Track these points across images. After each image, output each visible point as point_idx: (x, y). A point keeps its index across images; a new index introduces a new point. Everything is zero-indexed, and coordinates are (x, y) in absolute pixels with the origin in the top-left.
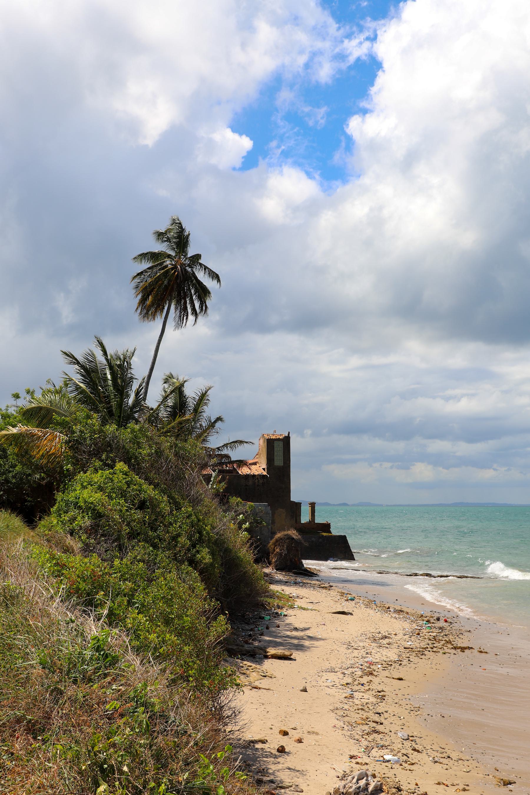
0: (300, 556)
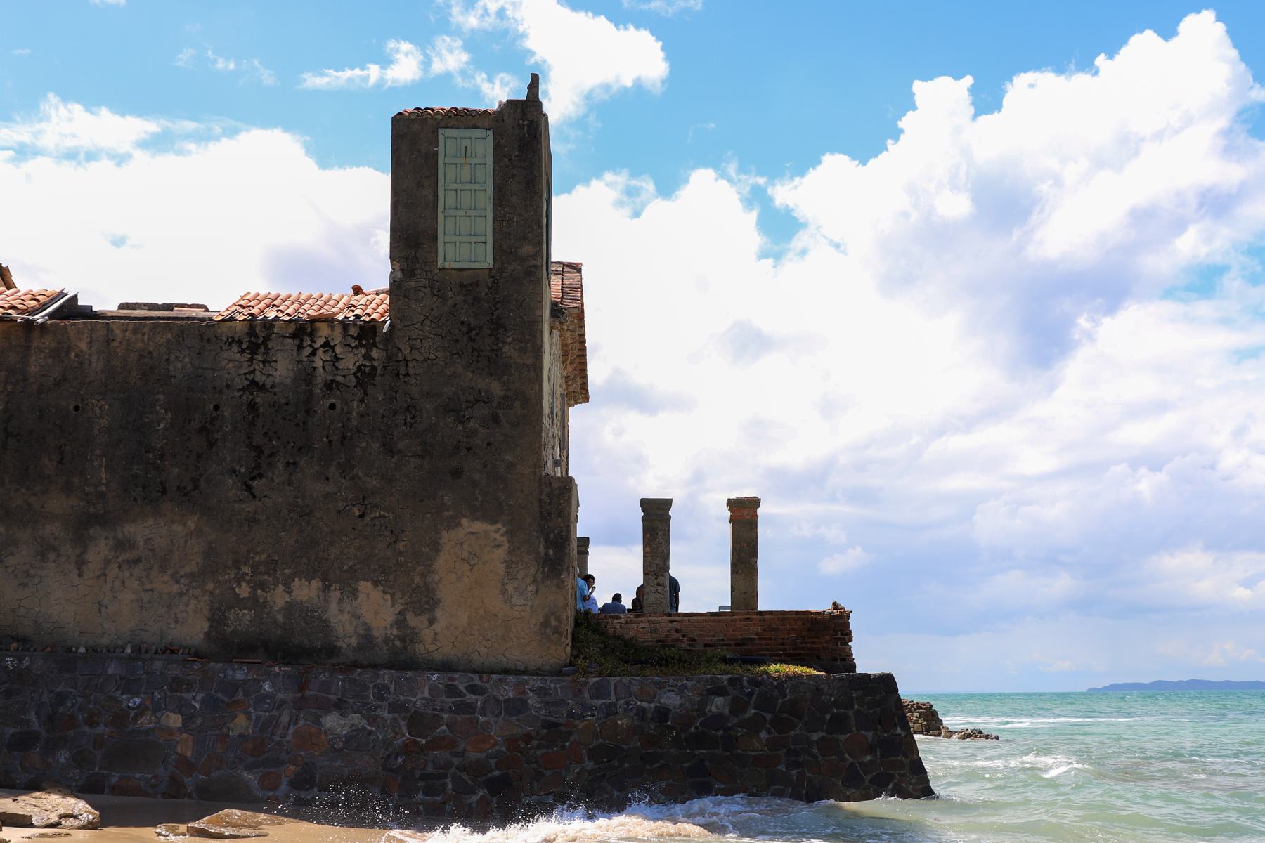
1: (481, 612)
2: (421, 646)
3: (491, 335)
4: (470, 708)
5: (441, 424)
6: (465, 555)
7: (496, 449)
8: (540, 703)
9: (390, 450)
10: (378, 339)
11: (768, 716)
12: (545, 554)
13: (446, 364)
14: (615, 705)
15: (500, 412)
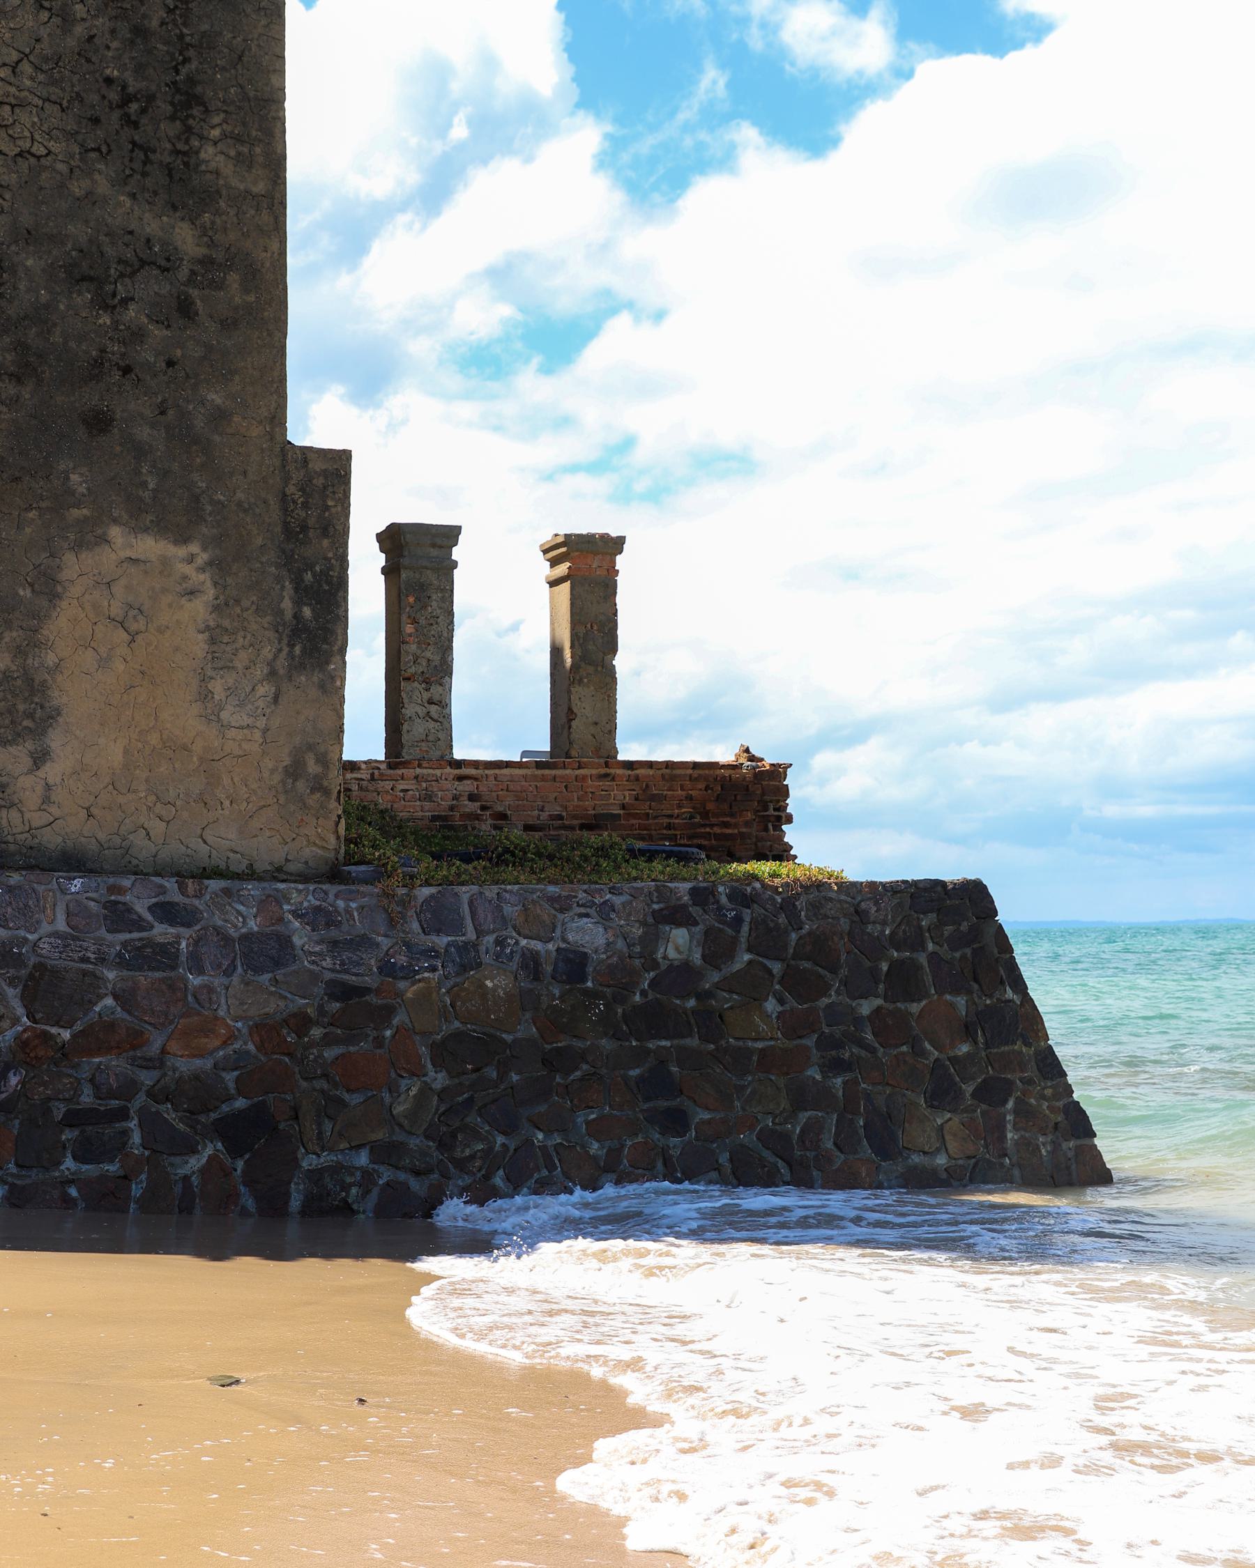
1: (154, 739)
2: (14, 814)
3: (173, 118)
4: (164, 956)
5: (62, 307)
6: (117, 610)
7: (188, 376)
8: (318, 943)
11: (776, 968)
12: (295, 616)
13: (71, 170)
14: (475, 946)
15: (194, 293)
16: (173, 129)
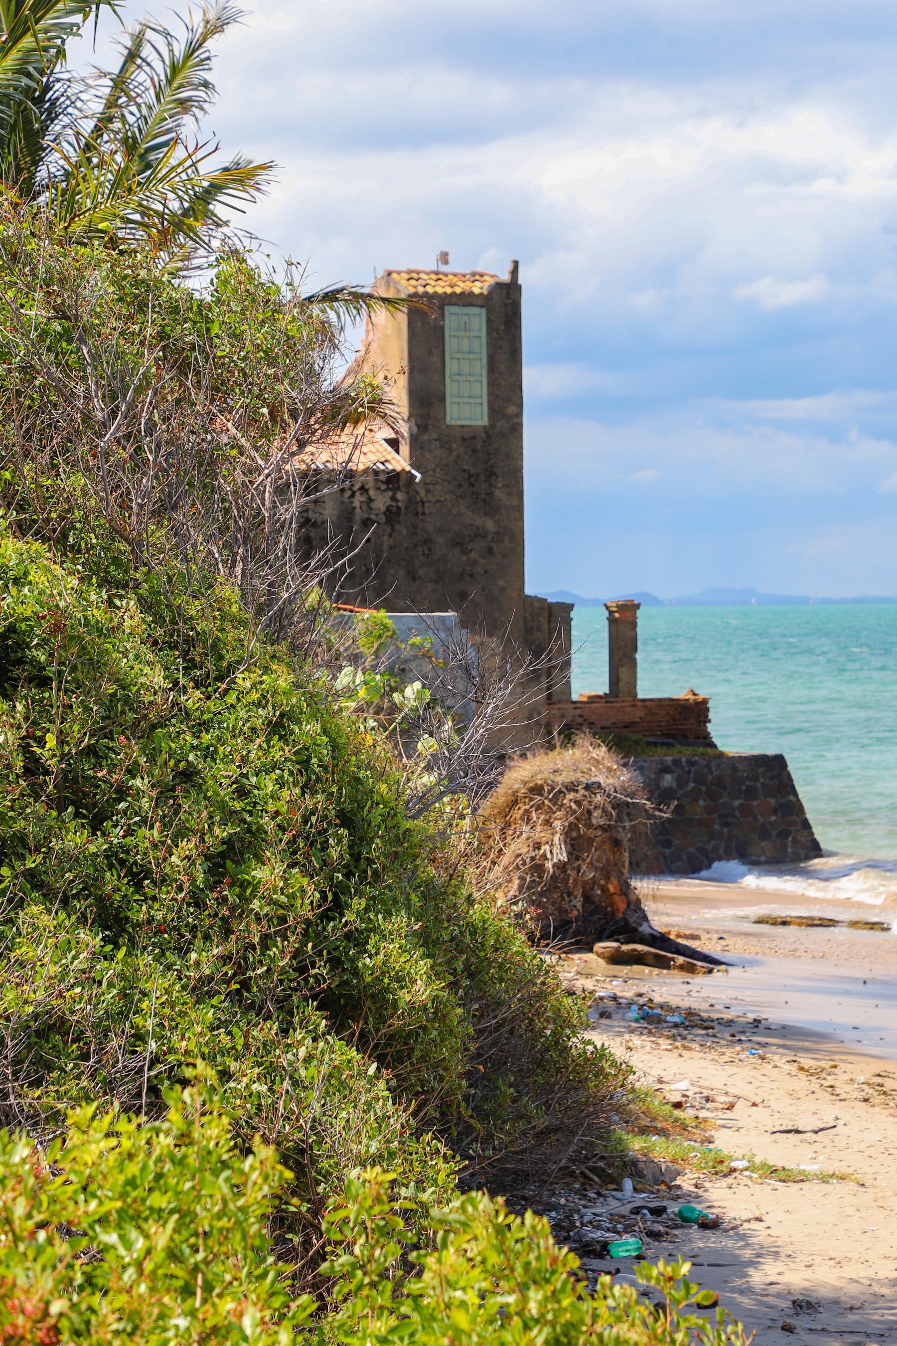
0: (626, 871)
9: (413, 577)
10: (401, 484)
11: (703, 789)
15: (494, 545)
16: (485, 485)
